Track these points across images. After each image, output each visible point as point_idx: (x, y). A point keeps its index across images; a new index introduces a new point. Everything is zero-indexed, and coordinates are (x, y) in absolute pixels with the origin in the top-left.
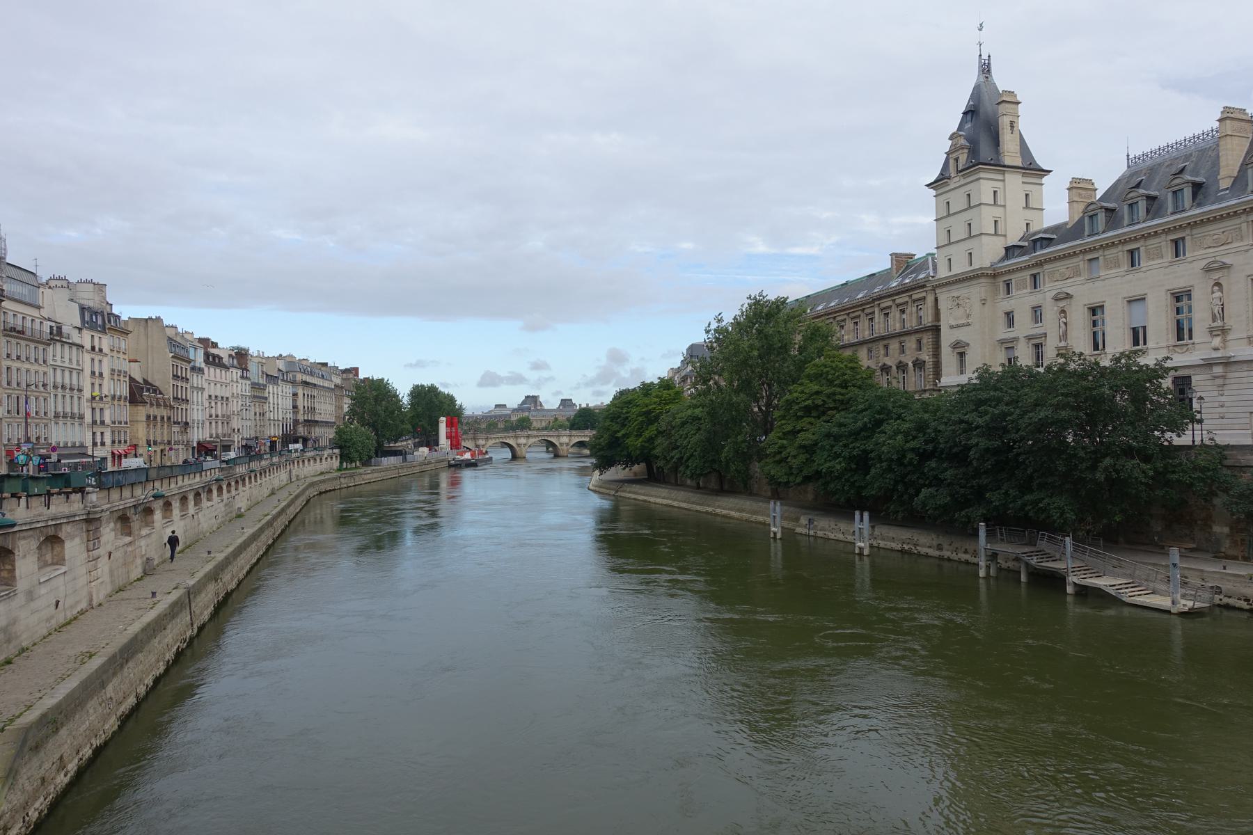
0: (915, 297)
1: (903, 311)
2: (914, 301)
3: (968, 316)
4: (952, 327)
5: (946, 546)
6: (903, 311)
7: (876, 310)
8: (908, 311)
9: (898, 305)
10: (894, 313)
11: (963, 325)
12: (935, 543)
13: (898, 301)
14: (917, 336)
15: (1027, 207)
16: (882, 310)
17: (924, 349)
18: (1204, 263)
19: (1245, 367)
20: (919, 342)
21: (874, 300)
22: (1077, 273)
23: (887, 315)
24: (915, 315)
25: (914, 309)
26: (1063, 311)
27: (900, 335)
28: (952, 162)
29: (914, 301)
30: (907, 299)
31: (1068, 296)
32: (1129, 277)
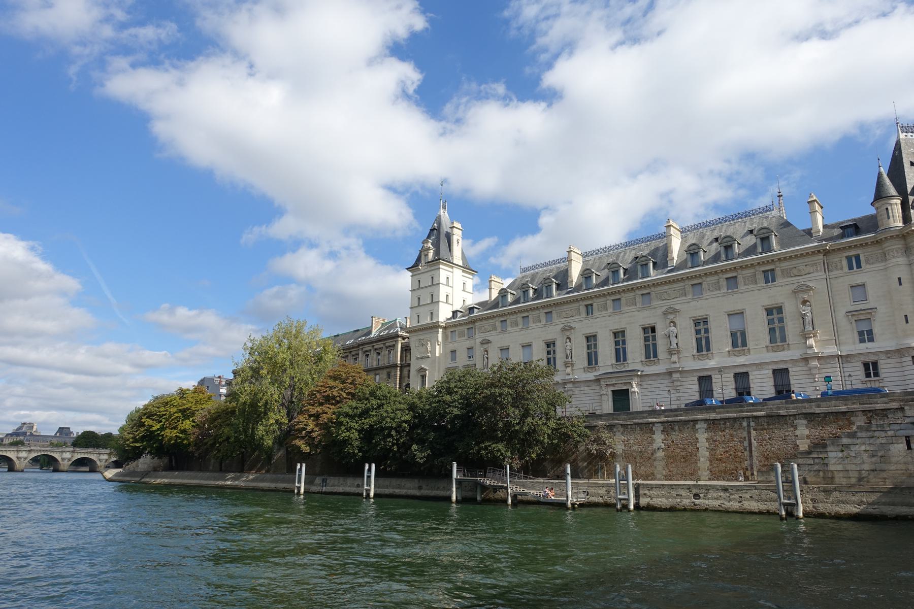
0: (387, 344)
1: (379, 354)
2: (387, 347)
4: (418, 359)
5: (424, 487)
6: (379, 354)
7: (360, 352)
8: (382, 354)
9: (376, 350)
10: (373, 355)
12: (417, 486)
15: (464, 290)
16: (364, 352)
18: (561, 326)
19: (582, 384)
21: (359, 346)
22: (495, 328)
23: (367, 356)
26: (486, 351)
28: (423, 256)
29: (387, 347)
31: (489, 342)
32: (523, 332)
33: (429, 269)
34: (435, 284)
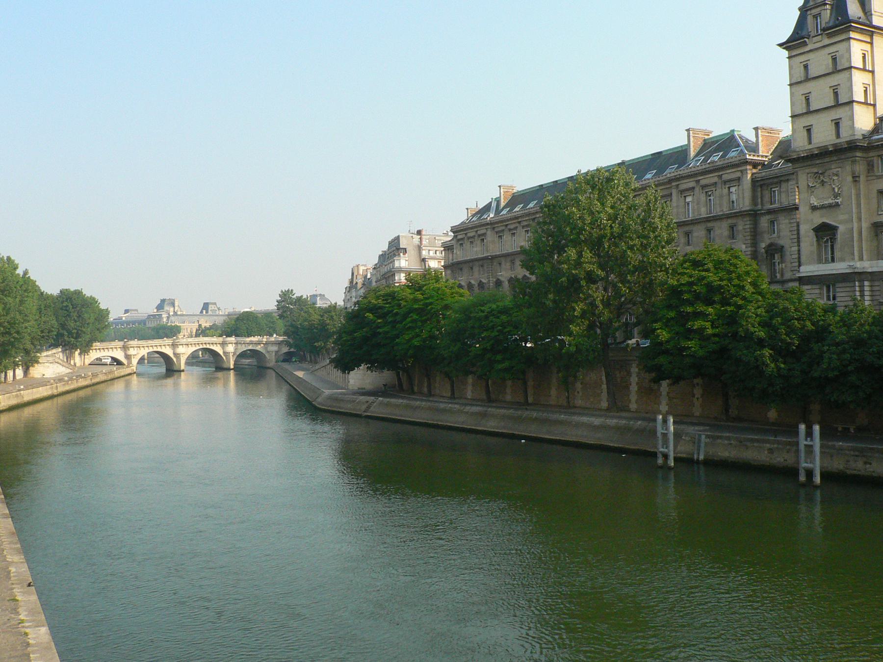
0: (726, 177)
2: (725, 182)
3: (836, 196)
4: (814, 208)
7: (674, 192)
9: (703, 187)
11: (830, 206)
13: (703, 182)
14: (730, 221)
17: (740, 236)
20: (732, 227)
24: (725, 199)
25: (725, 191)
27: (708, 220)
28: (810, 19)
30: (716, 179)
33: (827, 41)
34: (840, 68)
